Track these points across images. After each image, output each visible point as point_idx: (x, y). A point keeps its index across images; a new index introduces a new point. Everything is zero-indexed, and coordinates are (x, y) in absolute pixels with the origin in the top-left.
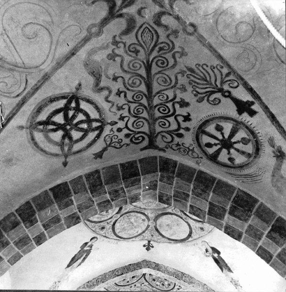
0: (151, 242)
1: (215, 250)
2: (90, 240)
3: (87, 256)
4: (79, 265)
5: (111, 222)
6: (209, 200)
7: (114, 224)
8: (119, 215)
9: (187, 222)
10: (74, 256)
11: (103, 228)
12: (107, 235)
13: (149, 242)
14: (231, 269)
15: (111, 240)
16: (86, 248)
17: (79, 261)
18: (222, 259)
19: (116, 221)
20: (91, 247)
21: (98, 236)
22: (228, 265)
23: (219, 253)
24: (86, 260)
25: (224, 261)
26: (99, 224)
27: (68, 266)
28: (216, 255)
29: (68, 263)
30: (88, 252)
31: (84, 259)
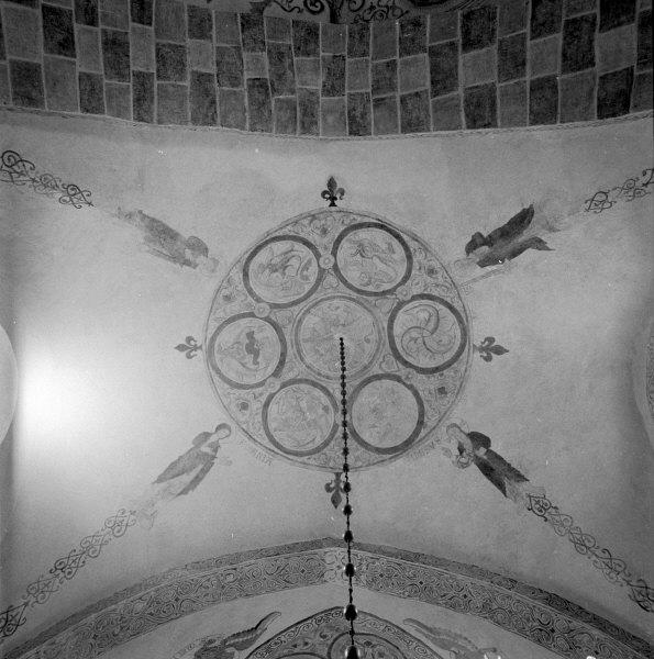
1: (480, 440)
3: (205, 471)
4: (181, 493)
5: (261, 395)
6: (428, 45)
7: (267, 405)
9: (410, 387)
11: (244, 406)
12: (251, 431)
14: (522, 473)
15: (260, 450)
16: (205, 449)
19: (271, 396)
20: (216, 451)
21: (233, 426)
22: (514, 465)
24: (200, 486)
26: (238, 392)
27: (160, 480)
28: (482, 452)
31: (197, 480)
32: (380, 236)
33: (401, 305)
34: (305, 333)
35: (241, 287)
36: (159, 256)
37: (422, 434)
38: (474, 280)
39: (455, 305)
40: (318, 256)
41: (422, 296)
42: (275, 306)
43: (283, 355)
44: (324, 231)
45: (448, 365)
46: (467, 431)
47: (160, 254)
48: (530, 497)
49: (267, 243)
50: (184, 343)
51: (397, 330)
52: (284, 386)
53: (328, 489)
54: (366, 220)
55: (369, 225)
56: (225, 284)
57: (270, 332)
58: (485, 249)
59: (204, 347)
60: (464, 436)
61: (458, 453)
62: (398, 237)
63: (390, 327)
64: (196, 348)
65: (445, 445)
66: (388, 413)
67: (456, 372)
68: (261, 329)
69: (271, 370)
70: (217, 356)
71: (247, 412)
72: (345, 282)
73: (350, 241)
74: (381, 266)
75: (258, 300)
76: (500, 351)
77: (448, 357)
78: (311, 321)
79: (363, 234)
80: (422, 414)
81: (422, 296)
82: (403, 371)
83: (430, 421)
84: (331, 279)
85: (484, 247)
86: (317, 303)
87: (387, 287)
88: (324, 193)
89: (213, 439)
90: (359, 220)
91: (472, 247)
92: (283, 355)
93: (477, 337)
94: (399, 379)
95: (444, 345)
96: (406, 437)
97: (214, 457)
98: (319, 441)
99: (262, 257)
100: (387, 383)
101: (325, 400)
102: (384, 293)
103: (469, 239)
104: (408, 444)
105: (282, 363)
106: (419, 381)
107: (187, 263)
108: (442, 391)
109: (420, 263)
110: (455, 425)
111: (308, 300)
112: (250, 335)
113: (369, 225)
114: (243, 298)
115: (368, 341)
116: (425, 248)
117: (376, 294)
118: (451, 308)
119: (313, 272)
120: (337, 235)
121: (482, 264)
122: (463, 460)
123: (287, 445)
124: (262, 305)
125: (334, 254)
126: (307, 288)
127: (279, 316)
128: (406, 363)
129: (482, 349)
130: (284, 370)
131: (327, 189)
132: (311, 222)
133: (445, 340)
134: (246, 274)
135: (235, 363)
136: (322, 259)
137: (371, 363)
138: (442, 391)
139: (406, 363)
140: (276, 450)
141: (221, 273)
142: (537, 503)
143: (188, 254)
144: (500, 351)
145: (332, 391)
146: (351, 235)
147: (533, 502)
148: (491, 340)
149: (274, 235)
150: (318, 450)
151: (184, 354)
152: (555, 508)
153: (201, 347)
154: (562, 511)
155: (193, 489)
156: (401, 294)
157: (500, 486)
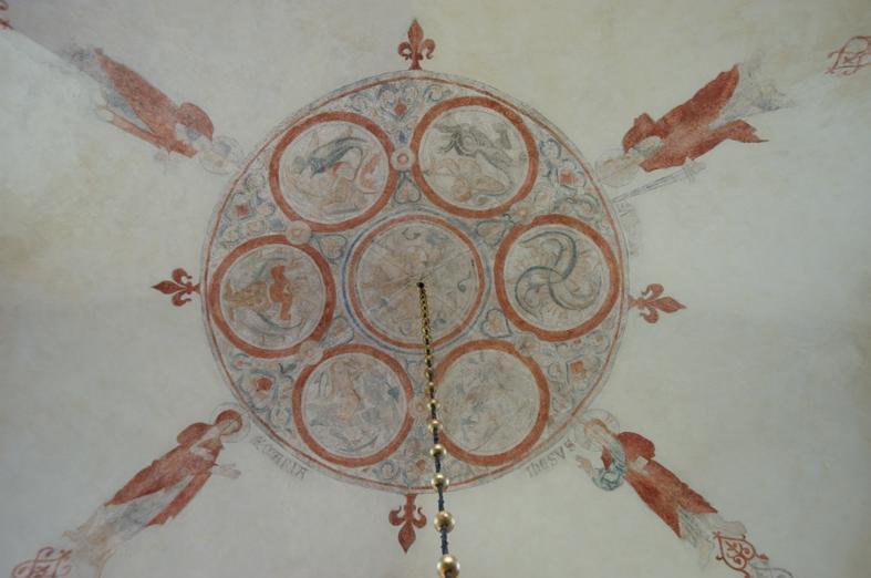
0: (417, 502)
1: (637, 444)
2: (215, 418)
3: (194, 488)
4: (154, 521)
5: (292, 367)
7: (301, 383)
8: (318, 352)
9: (529, 362)
10: (149, 464)
11: (264, 385)
13: (411, 498)
14: (707, 498)
15: (288, 453)
16: (197, 450)
17: (164, 498)
18: (664, 471)
20: (215, 453)
21: (246, 416)
23: (646, 448)
25: (671, 476)
27: (119, 498)
28: (640, 464)
29: (120, 486)
30: (203, 469)
31: (181, 501)
32: (488, 120)
33: (516, 231)
34: (364, 276)
35: (267, 194)
36: (131, 131)
37: (545, 435)
38: (635, 192)
39: (602, 232)
40: (389, 148)
41: (550, 218)
42: (318, 229)
43: (330, 305)
44: (401, 110)
45: (589, 326)
46: (617, 432)
47: (133, 129)
48: (720, 538)
49: (309, 122)
50: (169, 278)
51: (511, 269)
52: (328, 355)
53: (394, 519)
54: (471, 93)
55: (472, 101)
56: (240, 187)
57: (308, 263)
58: (655, 142)
59: (202, 288)
60: (611, 439)
61: (601, 465)
62: (516, 121)
63: (499, 267)
64: (190, 289)
65: (585, 453)
66: (492, 402)
67: (600, 339)
68: (296, 264)
69: (309, 328)
70: (223, 303)
71: (270, 393)
72: (430, 194)
73: (441, 128)
74: (489, 169)
75: (293, 216)
76: (671, 306)
77: (586, 316)
78: (375, 255)
79: (462, 117)
80: (545, 404)
81: (550, 218)
82: (518, 336)
83: (559, 413)
84: (409, 188)
85: (652, 138)
86: (384, 226)
87: (494, 203)
88: (403, 46)
89: (212, 434)
90: (457, 92)
91: (632, 138)
92: (330, 305)
93: (637, 281)
94: (510, 349)
95: (583, 296)
96: (520, 438)
97: (213, 464)
98: (382, 443)
99: (301, 146)
100: (491, 353)
101: (393, 380)
102: (490, 213)
103: (630, 125)
104: (525, 447)
105: (327, 319)
106: (543, 353)
107: (181, 149)
108: (577, 366)
109: (549, 164)
110: (599, 422)
111: (373, 221)
112: (278, 273)
113: (472, 101)
114: (268, 211)
115: (462, 289)
116: (559, 142)
117: (479, 214)
118: (596, 237)
119: (380, 175)
120: (421, 116)
121: (649, 166)
122: (611, 477)
123: (332, 451)
124: (298, 224)
125: (415, 148)
126: (372, 201)
127: (327, 245)
128: (521, 324)
129: (643, 303)
130: (331, 330)
131: (407, 40)
132: (381, 91)
133: (585, 289)
134: (274, 174)
135: (252, 317)
136: (395, 156)
137: (466, 323)
138: (577, 366)
139: (521, 324)
140: (314, 456)
141: (232, 169)
142: (732, 548)
143: (180, 132)
144: (671, 306)
145: (403, 366)
146: (440, 119)
147: (725, 547)
148: (657, 289)
149: (319, 112)
150: (380, 457)
151: (168, 297)
152: (763, 557)
153: (197, 288)
154: (773, 563)
155: (174, 515)
156: (521, 211)
157: (671, 520)
